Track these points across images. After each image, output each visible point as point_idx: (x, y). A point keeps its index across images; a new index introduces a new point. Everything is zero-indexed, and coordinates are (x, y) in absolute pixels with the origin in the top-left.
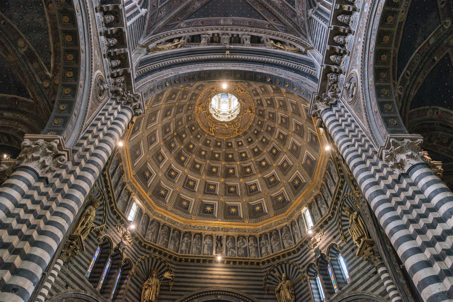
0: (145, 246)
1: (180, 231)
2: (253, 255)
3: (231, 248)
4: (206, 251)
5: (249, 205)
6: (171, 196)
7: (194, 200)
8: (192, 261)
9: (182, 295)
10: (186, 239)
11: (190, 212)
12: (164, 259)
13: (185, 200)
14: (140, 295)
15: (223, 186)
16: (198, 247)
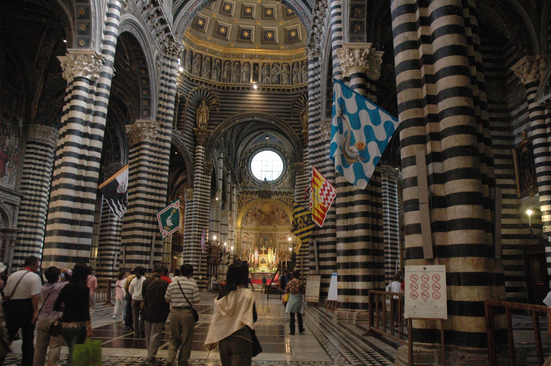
0: (193, 80)
1: (220, 60)
2: (285, 82)
3: (266, 75)
4: (244, 79)
5: (285, 29)
6: (209, 25)
7: (231, 25)
8: (233, 88)
9: (227, 118)
10: (226, 67)
11: (229, 39)
12: (209, 89)
13: (222, 26)
14: (195, 119)
15: (260, 8)
16: (238, 75)
